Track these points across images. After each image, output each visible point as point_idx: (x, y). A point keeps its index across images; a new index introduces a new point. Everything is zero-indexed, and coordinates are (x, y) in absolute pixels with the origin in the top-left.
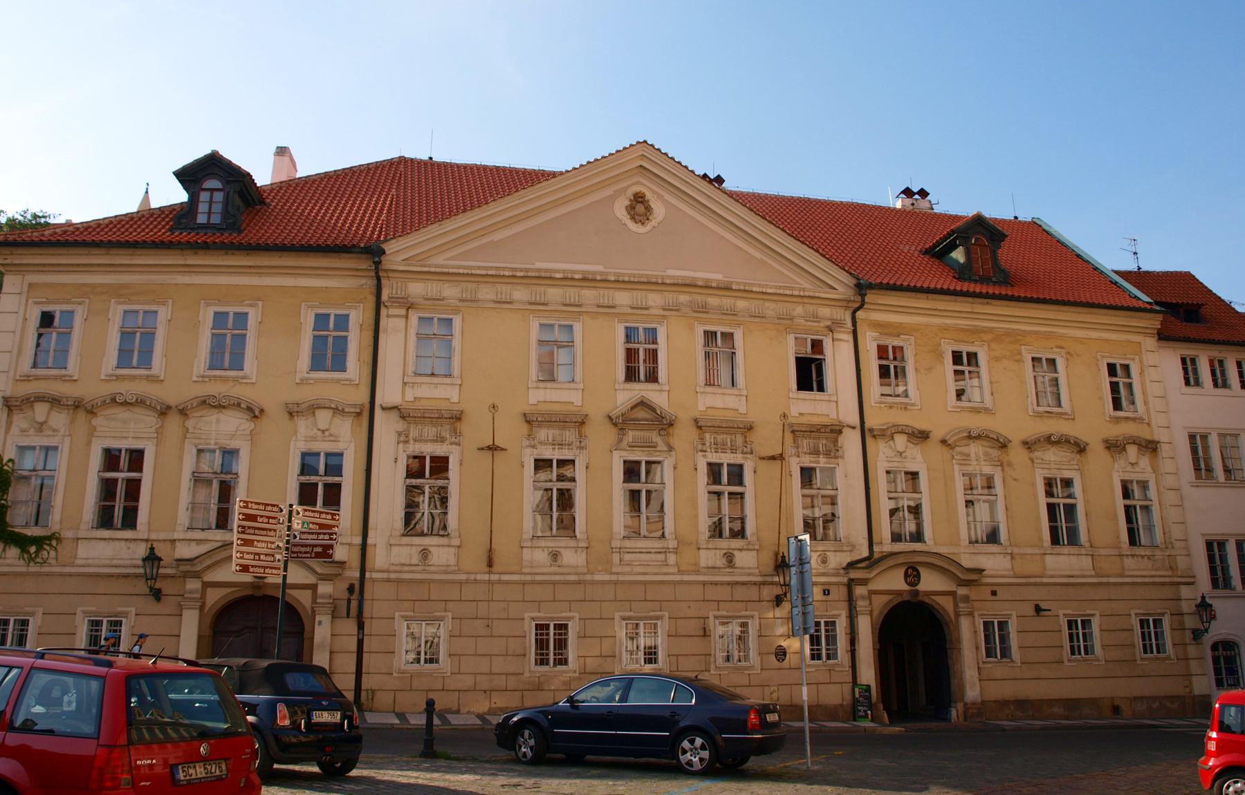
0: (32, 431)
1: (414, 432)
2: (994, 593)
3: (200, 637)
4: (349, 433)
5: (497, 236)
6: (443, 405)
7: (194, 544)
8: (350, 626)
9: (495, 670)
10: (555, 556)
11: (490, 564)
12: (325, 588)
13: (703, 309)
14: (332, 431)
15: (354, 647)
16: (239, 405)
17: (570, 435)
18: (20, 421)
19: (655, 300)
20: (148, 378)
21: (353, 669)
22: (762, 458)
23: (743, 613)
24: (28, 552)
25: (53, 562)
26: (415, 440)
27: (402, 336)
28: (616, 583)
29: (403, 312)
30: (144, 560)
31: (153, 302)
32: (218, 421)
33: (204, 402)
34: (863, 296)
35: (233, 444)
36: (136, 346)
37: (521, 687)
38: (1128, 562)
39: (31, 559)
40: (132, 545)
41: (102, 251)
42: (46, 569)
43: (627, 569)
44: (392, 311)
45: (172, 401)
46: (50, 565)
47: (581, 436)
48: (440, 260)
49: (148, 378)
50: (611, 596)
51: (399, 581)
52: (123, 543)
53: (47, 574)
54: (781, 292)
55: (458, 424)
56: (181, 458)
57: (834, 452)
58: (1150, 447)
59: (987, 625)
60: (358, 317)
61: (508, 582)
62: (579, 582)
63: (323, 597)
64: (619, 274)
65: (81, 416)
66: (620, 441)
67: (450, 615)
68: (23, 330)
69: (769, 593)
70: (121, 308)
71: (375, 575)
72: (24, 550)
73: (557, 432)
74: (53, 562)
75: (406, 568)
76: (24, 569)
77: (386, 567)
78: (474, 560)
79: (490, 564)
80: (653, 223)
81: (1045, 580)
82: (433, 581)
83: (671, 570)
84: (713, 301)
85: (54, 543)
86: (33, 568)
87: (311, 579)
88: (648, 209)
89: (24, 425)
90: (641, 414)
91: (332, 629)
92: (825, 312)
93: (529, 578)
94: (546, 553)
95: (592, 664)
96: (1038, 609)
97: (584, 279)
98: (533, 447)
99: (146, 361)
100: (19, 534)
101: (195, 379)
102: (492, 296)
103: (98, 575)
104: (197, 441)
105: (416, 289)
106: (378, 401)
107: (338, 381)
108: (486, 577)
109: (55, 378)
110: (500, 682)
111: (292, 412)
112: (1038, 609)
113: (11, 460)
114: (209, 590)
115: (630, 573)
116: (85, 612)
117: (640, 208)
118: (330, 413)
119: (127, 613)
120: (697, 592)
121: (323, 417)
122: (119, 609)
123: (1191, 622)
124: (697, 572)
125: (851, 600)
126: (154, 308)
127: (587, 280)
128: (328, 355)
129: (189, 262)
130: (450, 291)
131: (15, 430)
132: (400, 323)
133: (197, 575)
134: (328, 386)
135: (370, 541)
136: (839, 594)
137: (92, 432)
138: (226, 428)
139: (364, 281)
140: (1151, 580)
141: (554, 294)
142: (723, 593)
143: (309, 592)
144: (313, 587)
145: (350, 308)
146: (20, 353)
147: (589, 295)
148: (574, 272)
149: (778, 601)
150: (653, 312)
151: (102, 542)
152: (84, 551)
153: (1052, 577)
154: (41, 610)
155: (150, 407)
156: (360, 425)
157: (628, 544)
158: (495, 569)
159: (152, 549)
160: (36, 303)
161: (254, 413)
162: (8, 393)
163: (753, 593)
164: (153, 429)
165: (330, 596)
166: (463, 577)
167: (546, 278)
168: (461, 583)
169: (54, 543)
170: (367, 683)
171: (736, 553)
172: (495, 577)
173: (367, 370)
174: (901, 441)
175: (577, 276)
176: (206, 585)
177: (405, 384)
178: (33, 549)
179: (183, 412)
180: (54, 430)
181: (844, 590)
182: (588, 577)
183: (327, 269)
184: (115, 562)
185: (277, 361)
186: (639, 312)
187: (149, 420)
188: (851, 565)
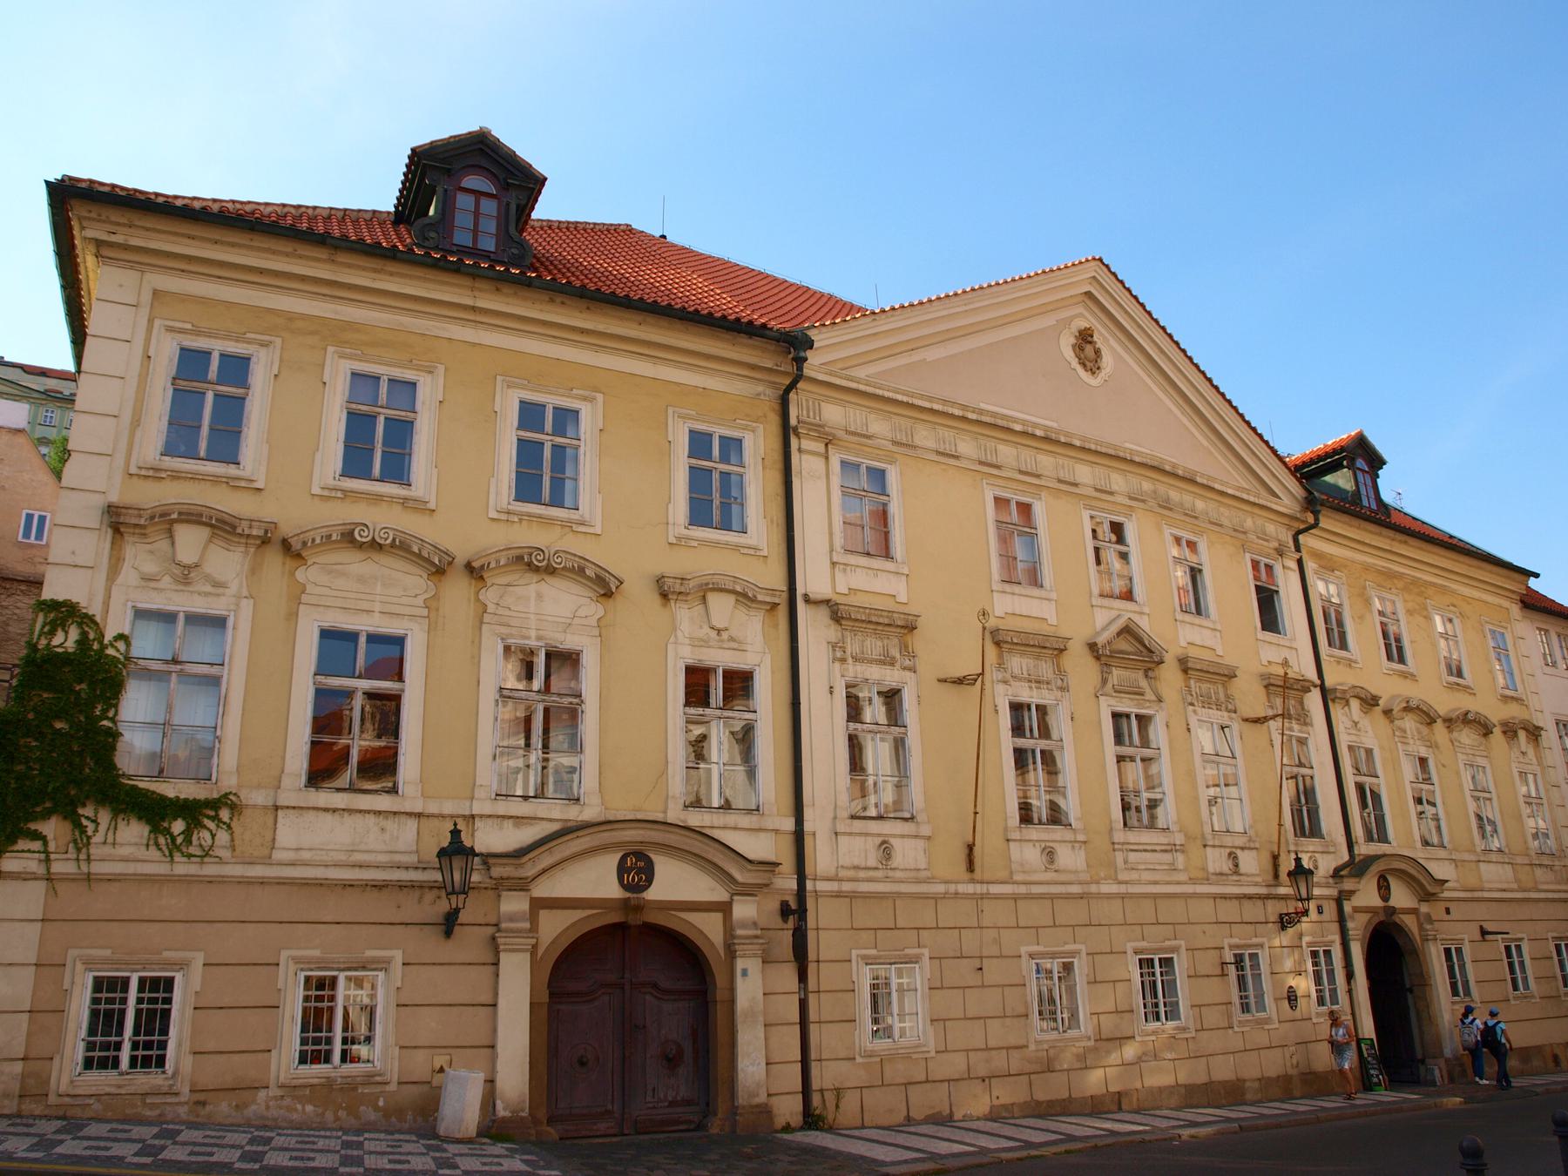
0: (166, 581)
1: (852, 646)
2: (1448, 911)
3: (533, 1006)
4: (760, 638)
6: (888, 605)
7: (509, 824)
8: (787, 977)
9: (992, 1044)
10: (1050, 854)
11: (971, 867)
12: (744, 910)
13: (1166, 505)
14: (734, 632)
15: (795, 1016)
16: (581, 570)
17: (1046, 669)
18: (140, 557)
19: (1119, 481)
20: (405, 502)
21: (796, 1054)
22: (1246, 720)
23: (1255, 940)
24: (168, 832)
25: (225, 854)
26: (856, 659)
27: (822, 484)
28: (1123, 897)
29: (820, 447)
30: (442, 853)
31: (409, 364)
32: (539, 596)
33: (520, 558)
34: (1316, 513)
35: (569, 642)
36: (378, 441)
37: (1028, 1068)
38: (1539, 872)
39: (174, 847)
40: (390, 824)
41: (322, 253)
42: (210, 870)
43: (1134, 876)
44: (806, 444)
47: (1060, 672)
48: (861, 373)
49: (405, 502)
50: (1119, 918)
51: (852, 896)
52: (371, 819)
53: (210, 881)
54: (1238, 494)
55: (909, 638)
56: (476, 661)
57: (1304, 719)
58: (1535, 733)
59: (1448, 951)
60: (758, 444)
61: (998, 897)
62: (1081, 897)
63: (744, 925)
64: (1084, 439)
65: (274, 561)
66: (1104, 681)
67: (926, 952)
68: (144, 377)
69: (1274, 909)
70: (347, 366)
71: (822, 886)
72: (156, 829)
73: (1031, 662)
74: (225, 854)
75: (862, 874)
76: (162, 869)
77: (832, 872)
78: (950, 862)
79: (971, 867)
80: (1103, 374)
81: (1486, 895)
82: (899, 895)
83: (1183, 877)
84: (1174, 495)
85: (225, 814)
86: (182, 867)
87: (719, 894)
88: (1097, 352)
89: (150, 567)
90: (1124, 645)
91: (764, 985)
92: (1271, 528)
93: (1022, 889)
94: (1038, 850)
96: (1484, 932)
97: (1046, 439)
98: (1005, 682)
99: (397, 470)
100: (146, 793)
101: (493, 514)
102: (931, 444)
103: (320, 884)
104: (504, 630)
105: (833, 414)
106: (800, 591)
107: (737, 548)
108: (970, 888)
109: (216, 480)
110: (999, 1061)
111: (666, 592)
112: (1484, 932)
114: (543, 914)
115: (1139, 882)
116: (297, 960)
117: (1089, 349)
118: (731, 599)
119: (388, 961)
120: (1205, 910)
121: (721, 605)
122: (370, 953)
124: (1207, 880)
125: (1341, 920)
126: (409, 375)
128: (712, 502)
129: (481, 304)
130: (879, 426)
131: (128, 576)
132: (816, 464)
133: (522, 885)
134: (709, 555)
135: (808, 827)
136: (1330, 910)
137: (297, 595)
138: (553, 611)
139: (760, 389)
140: (1556, 896)
141: (1007, 453)
142: (1229, 911)
143: (717, 917)
144: (725, 908)
145: (745, 428)
146: (136, 422)
147: (1046, 462)
148: (1035, 425)
149: (1285, 922)
150: (1119, 499)
151: (328, 816)
152: (290, 832)
153: (1490, 890)
154: (199, 959)
155: (420, 559)
156: (776, 626)
157: (1132, 837)
158: (978, 875)
159: (456, 833)
160: (170, 329)
161: (605, 588)
162: (114, 498)
163: (1252, 911)
164: (420, 601)
165: (755, 924)
166: (941, 888)
167: (1000, 428)
168: (936, 898)
169: (225, 814)
170: (823, 1076)
171: (1239, 852)
172: (979, 889)
173: (778, 535)
175: (1039, 433)
176: (538, 904)
177: (834, 564)
178: (178, 826)
179: (475, 572)
180: (217, 584)
181: (1333, 905)
182: (1093, 888)
183: (708, 357)
184: (358, 857)
185: (627, 497)
186: (1104, 496)
187: (411, 582)
188: (1337, 874)
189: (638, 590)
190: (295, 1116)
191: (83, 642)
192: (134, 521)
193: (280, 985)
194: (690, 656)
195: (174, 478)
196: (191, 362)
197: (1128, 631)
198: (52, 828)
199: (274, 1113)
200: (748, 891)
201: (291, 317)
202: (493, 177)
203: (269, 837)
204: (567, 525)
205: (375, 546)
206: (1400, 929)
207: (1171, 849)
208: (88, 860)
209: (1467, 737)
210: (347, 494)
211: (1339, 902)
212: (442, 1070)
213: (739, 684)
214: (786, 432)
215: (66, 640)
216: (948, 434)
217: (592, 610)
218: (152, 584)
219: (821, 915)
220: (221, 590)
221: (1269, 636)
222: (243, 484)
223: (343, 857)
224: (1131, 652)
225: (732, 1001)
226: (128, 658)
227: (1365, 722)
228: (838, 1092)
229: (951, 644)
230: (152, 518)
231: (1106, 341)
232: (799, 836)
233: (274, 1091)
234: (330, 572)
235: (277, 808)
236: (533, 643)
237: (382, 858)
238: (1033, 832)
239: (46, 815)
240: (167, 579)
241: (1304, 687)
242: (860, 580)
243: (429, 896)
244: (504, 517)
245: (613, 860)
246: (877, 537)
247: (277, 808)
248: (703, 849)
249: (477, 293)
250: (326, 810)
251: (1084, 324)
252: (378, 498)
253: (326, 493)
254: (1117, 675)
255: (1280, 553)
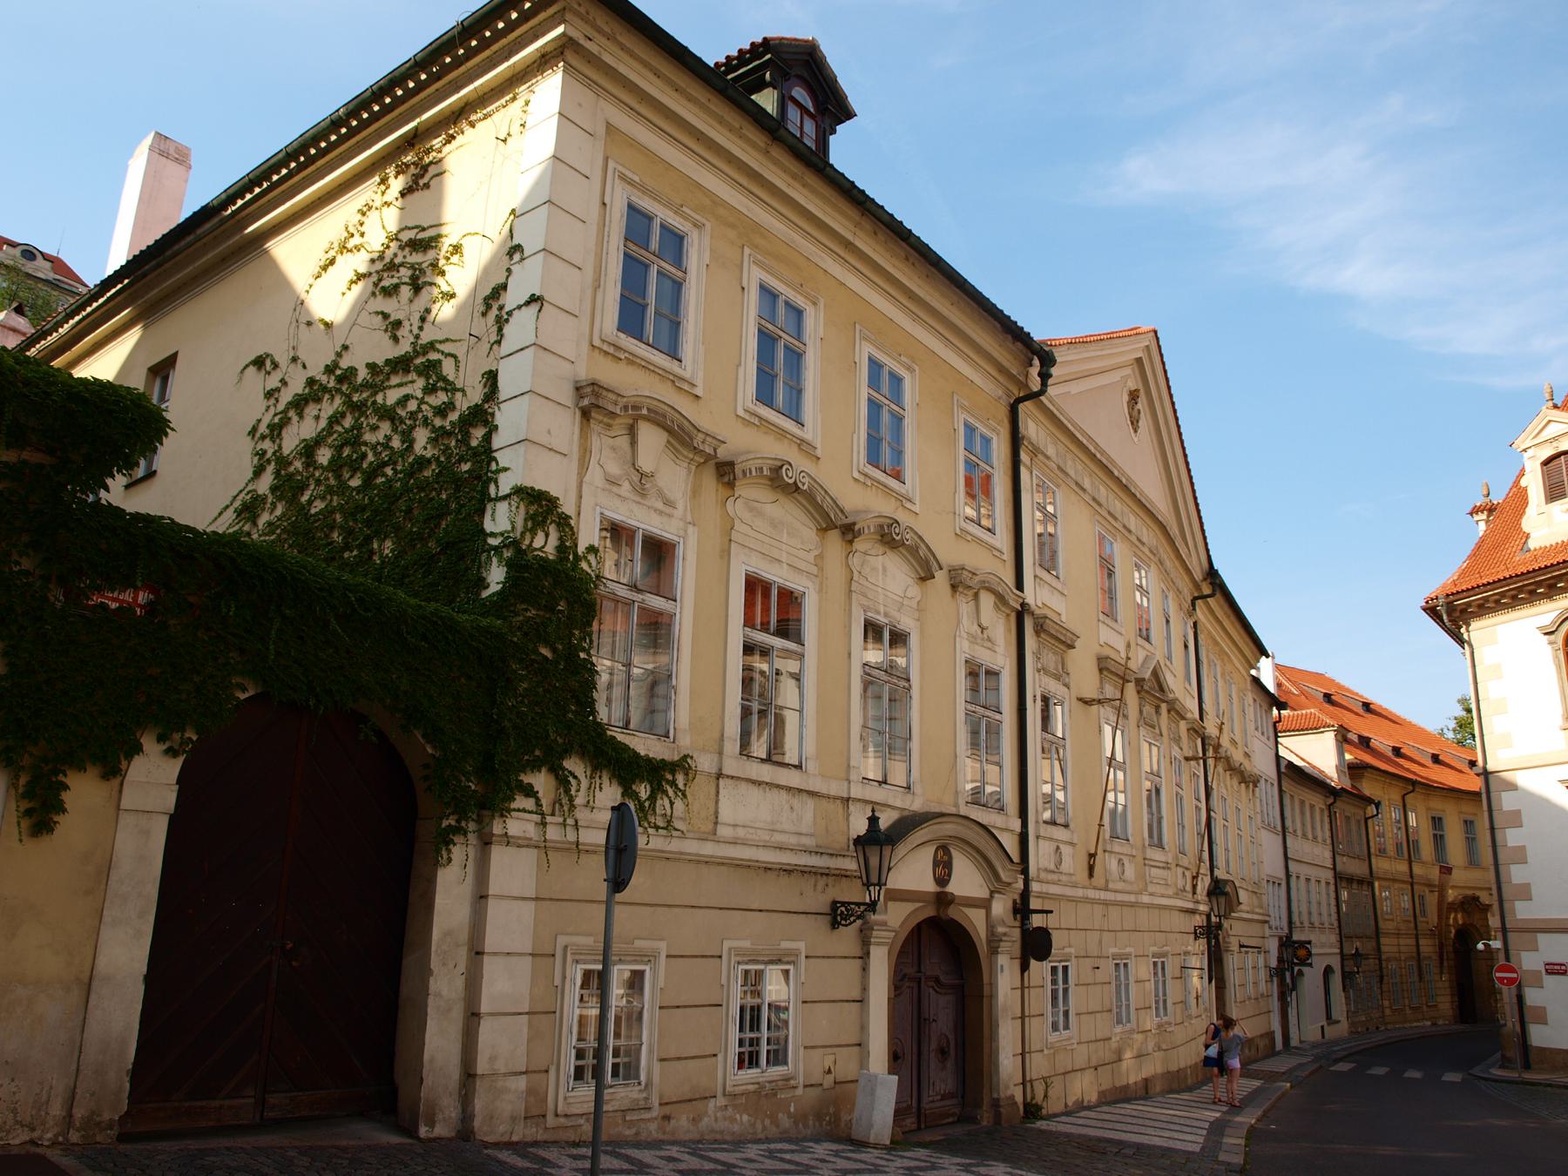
11: (1091, 875)
18: (607, 451)
30: (859, 841)
40: (796, 802)
41: (759, 138)
42: (675, 845)
46: (683, 835)
89: (614, 469)
113: (592, 549)
116: (739, 952)
122: (785, 945)
131: (594, 476)
143: (983, 912)
144: (986, 904)
162: (583, 374)
180: (669, 503)
190: (736, 1128)
191: (561, 549)
192: (611, 408)
193: (724, 981)
195: (630, 362)
196: (638, 221)
198: (541, 781)
199: (722, 1125)
201: (717, 202)
203: (712, 810)
205: (795, 489)
208: (576, 826)
212: (829, 1071)
215: (546, 544)
217: (914, 591)
218: (615, 489)
220: (668, 510)
222: (686, 387)
223: (765, 836)
225: (993, 996)
226: (598, 577)
228: (1046, 1081)
230: (626, 408)
233: (721, 1101)
234: (751, 510)
235: (719, 775)
236: (882, 619)
237: (793, 840)
239: (535, 766)
240: (626, 485)
243: (822, 881)
244: (862, 478)
247: (719, 775)
249: (859, 232)
250: (754, 782)
253: (747, 417)
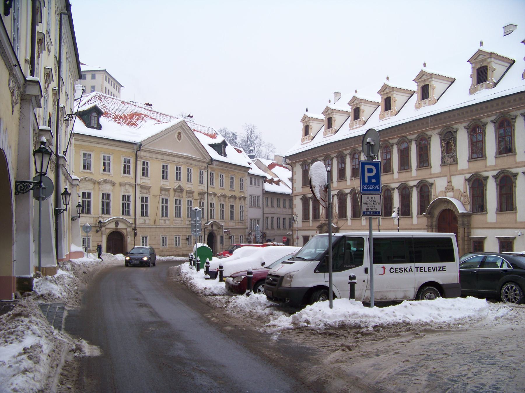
5: (156, 141)
10: (165, 221)
12: (129, 229)
17: (167, 193)
19: (181, 160)
31: (90, 151)
45: (97, 180)
47: (169, 194)
48: (146, 146)
57: (204, 199)
58: (244, 198)
60: (132, 160)
78: (152, 223)
95: (171, 246)
99: (89, 168)
107: (129, 177)
121: (127, 186)
123: (247, 237)
125: (205, 232)
127: (172, 155)
128: (126, 171)
130: (148, 155)
138: (107, 188)
141: (165, 157)
144: (126, 229)
147: (170, 158)
161: (114, 184)
174: (213, 196)
176: (107, 228)
189: (117, 185)
194: (122, 194)
197: (179, 186)
200: (129, 227)
202: (96, 113)
204: (109, 175)
206: (214, 233)
207: (181, 220)
209: (231, 200)
210: (84, 172)
211: (205, 229)
213: (129, 197)
214: (136, 157)
216: (157, 155)
217: (112, 188)
219: (138, 231)
221: (201, 185)
224: (179, 190)
227: (214, 198)
229: (155, 191)
231: (183, 135)
232: (135, 219)
238: (163, 218)
241: (205, 193)
242: (144, 181)
245: (114, 223)
246: (145, 173)
248: (124, 221)
251: (179, 131)
252: (87, 173)
254: (177, 194)
255: (205, 169)
